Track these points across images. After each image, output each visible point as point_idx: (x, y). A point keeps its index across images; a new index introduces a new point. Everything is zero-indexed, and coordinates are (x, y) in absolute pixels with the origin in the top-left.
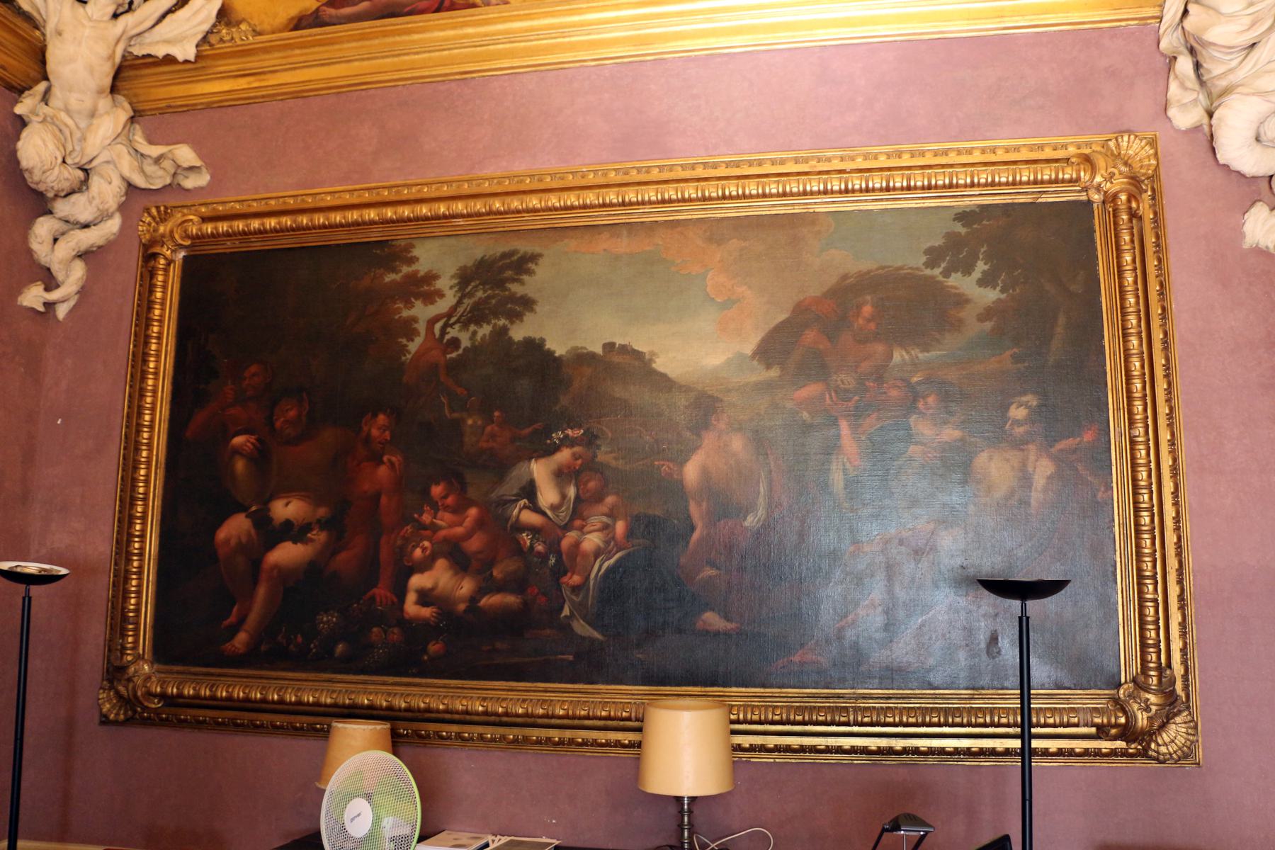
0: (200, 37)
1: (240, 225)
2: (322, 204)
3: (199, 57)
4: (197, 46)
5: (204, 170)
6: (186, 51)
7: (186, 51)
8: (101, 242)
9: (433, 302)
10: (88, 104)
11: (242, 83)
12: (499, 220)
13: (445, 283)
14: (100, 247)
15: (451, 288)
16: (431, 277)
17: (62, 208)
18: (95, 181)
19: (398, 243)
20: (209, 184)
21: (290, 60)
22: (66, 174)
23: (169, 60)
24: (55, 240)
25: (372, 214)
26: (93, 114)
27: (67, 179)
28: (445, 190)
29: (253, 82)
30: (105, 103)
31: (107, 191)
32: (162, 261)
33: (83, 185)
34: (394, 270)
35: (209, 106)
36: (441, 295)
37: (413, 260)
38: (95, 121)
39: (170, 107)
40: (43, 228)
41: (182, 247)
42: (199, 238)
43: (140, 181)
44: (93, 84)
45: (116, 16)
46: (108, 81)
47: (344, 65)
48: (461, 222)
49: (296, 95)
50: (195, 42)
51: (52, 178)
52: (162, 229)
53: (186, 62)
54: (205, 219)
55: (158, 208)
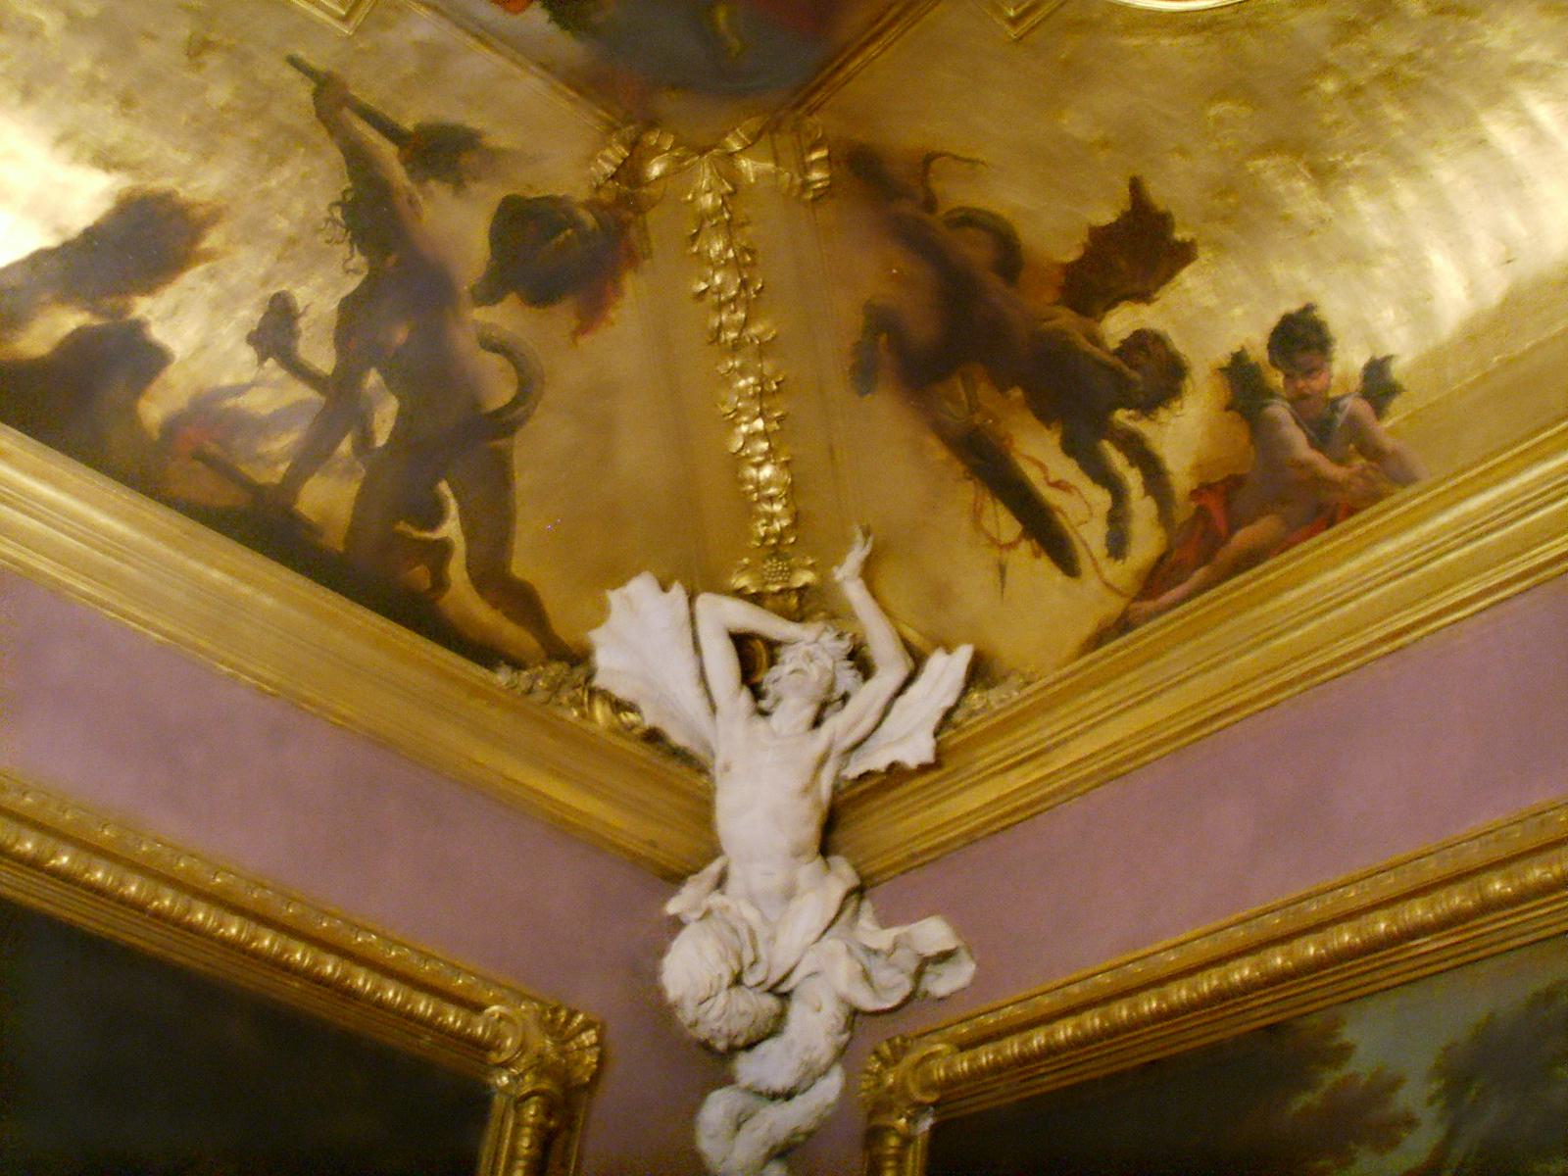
0: (937, 717)
1: (1012, 1047)
2: (1161, 972)
3: (940, 753)
4: (936, 734)
5: (963, 954)
6: (916, 750)
7: (916, 750)
8: (807, 1124)
9: (1394, 1143)
10: (779, 879)
11: (1015, 780)
12: (1511, 919)
13: (1415, 1096)
14: (809, 1134)
15: (1431, 1100)
16: (1385, 1086)
17: (750, 1068)
18: (797, 1012)
19: (1315, 1020)
20: (975, 980)
21: (1088, 712)
22: (743, 1005)
23: (896, 772)
24: (738, 1127)
25: (1242, 972)
26: (789, 893)
27: (744, 1014)
28: (1390, 884)
29: (1033, 773)
30: (808, 870)
31: (813, 1027)
32: (893, 1141)
33: (775, 1026)
34: (1308, 1086)
35: (971, 839)
36: (1410, 1122)
37: (1345, 1052)
38: (795, 904)
39: (914, 856)
40: (717, 1108)
41: (920, 1108)
42: (951, 1083)
43: (867, 1001)
44: (783, 841)
45: (817, 722)
46: (810, 832)
47: (1174, 693)
48: (1426, 944)
49: (1109, 776)
50: (931, 726)
51: (714, 1014)
52: (890, 1080)
53: (924, 769)
54: (965, 1046)
55: (889, 1041)
